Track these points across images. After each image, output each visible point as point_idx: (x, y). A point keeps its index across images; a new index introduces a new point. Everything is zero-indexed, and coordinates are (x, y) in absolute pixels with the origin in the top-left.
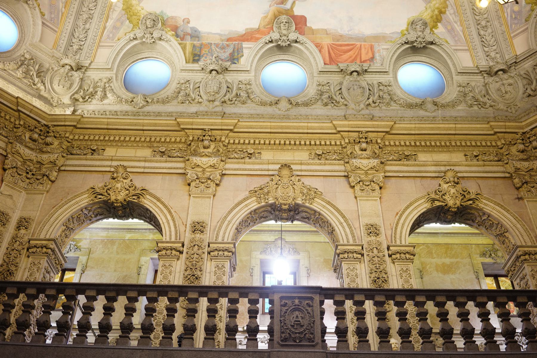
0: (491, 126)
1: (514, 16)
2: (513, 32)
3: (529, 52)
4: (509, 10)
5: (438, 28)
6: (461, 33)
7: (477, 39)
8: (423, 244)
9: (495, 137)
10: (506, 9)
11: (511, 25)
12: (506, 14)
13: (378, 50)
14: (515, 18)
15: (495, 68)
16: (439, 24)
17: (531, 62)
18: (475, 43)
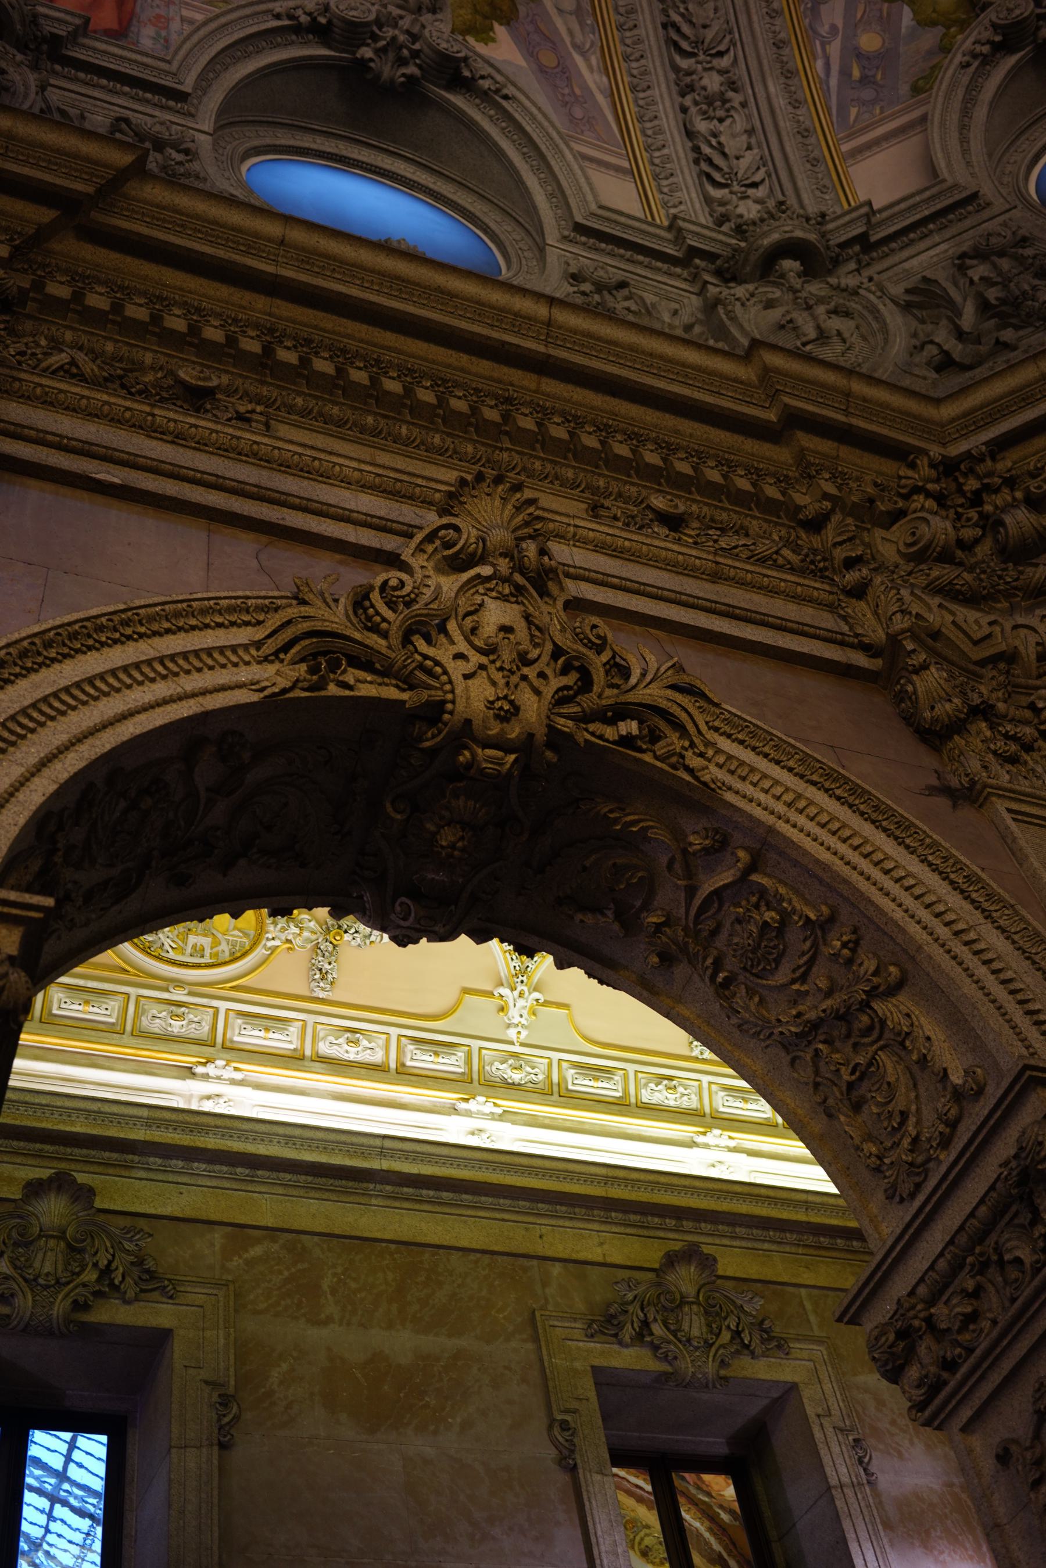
0: (767, 372)
1: (856, 73)
2: (850, 137)
3: (932, 198)
4: (835, 49)
5: (494, 40)
6: (602, 101)
7: (678, 148)
8: (273, 1232)
9: (781, 455)
10: (823, 45)
11: (842, 110)
12: (820, 64)
13: (159, 17)
14: (865, 80)
15: (765, 235)
16: (500, 31)
17: (943, 247)
18: (666, 151)
